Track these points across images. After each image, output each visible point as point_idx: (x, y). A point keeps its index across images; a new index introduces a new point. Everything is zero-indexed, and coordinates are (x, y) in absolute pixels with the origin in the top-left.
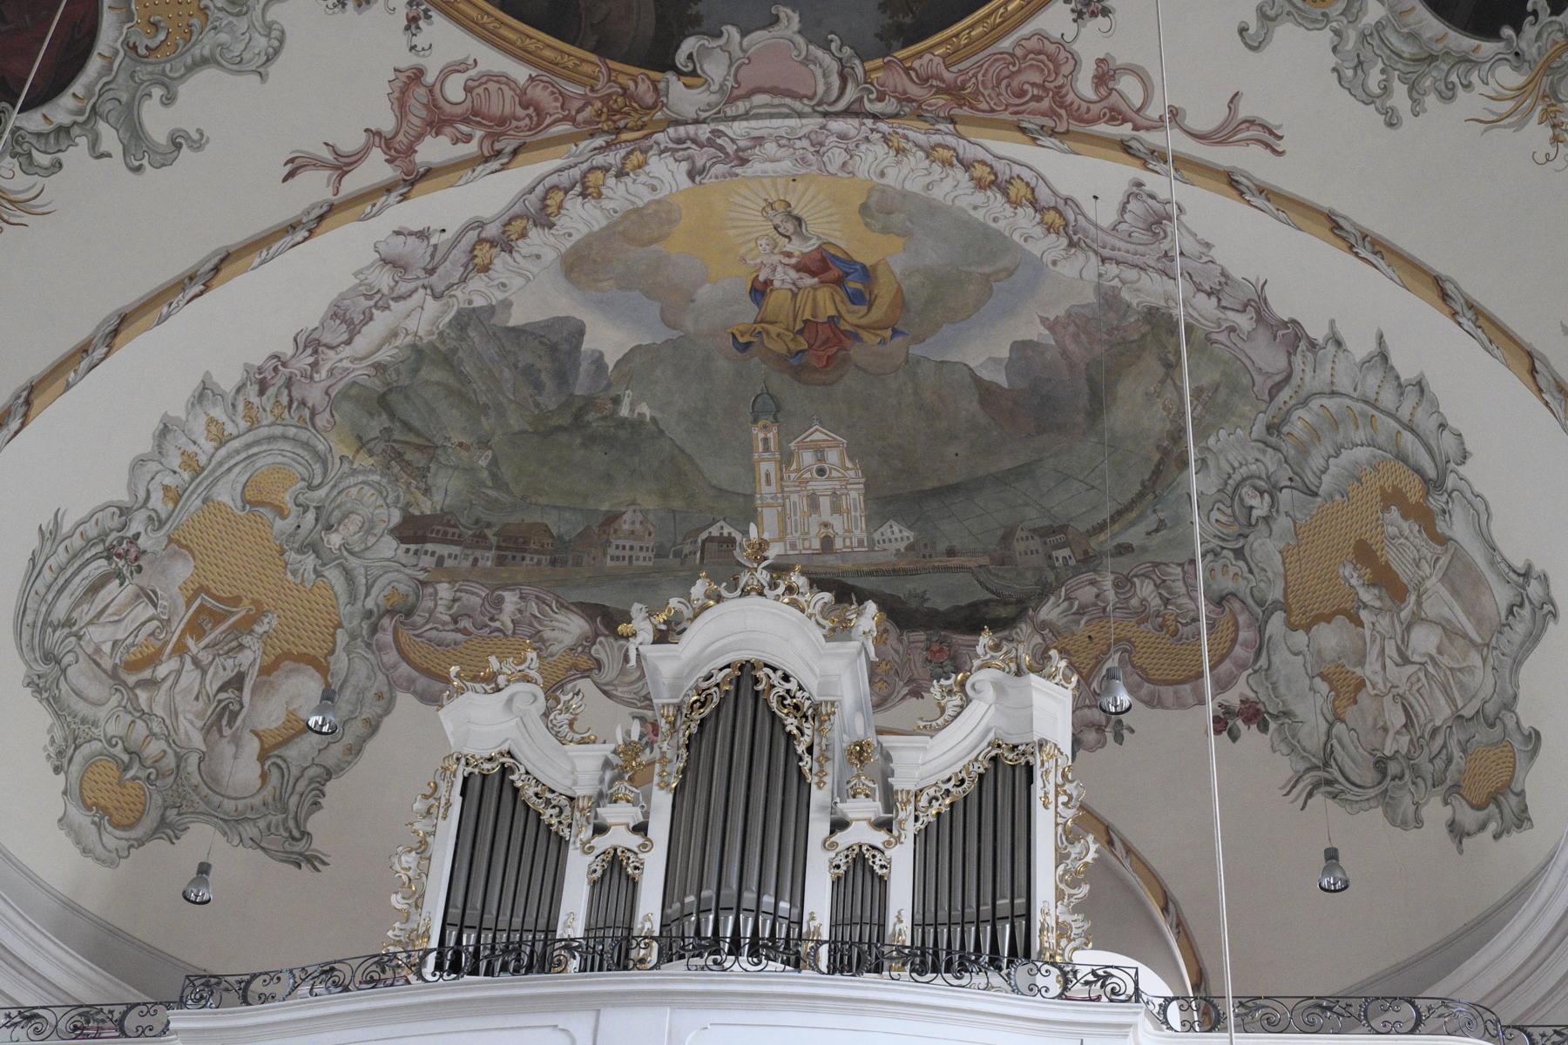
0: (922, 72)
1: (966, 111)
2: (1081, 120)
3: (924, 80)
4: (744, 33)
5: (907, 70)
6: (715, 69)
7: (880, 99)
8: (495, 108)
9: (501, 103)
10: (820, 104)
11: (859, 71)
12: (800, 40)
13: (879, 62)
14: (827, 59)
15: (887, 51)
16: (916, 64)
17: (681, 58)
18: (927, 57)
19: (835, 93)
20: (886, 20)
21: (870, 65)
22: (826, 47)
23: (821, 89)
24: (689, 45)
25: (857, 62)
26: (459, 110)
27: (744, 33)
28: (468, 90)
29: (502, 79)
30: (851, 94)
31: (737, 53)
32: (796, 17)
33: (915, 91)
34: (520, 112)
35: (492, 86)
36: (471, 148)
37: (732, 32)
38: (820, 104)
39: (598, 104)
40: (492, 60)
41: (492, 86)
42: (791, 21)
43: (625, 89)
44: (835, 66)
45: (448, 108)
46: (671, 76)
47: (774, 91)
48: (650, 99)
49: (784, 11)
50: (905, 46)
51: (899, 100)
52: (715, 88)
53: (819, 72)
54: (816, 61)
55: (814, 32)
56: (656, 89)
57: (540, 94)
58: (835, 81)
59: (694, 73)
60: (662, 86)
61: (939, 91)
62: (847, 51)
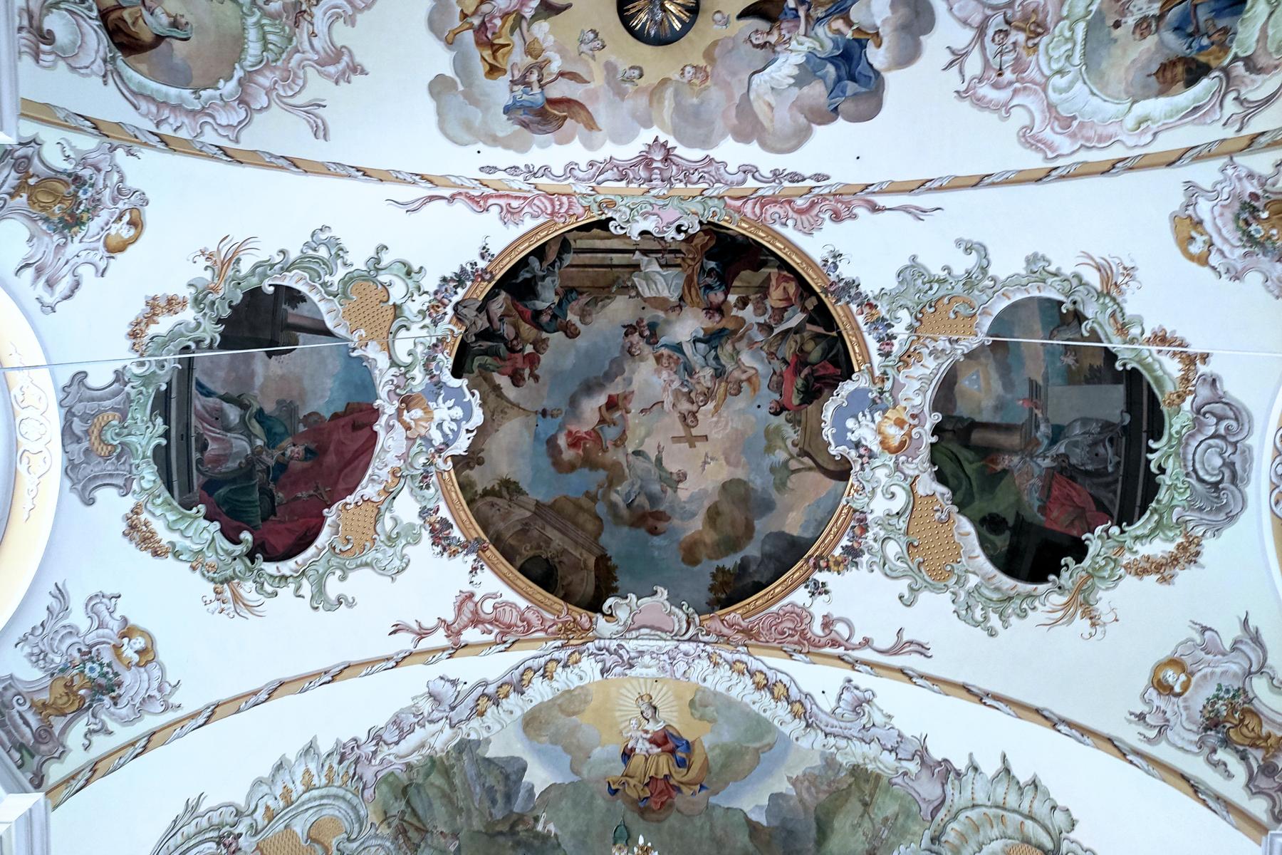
0: (730, 622)
1: (753, 641)
2: (815, 646)
3: (731, 626)
4: (639, 599)
5: (722, 621)
6: (622, 614)
7: (708, 634)
10: (675, 635)
11: (697, 620)
12: (667, 604)
13: (708, 616)
14: (680, 613)
15: (713, 611)
16: (727, 618)
17: (605, 607)
18: (733, 615)
19: (684, 631)
20: (711, 596)
21: (702, 617)
22: (680, 607)
23: (676, 628)
24: (610, 601)
25: (696, 616)
27: (639, 599)
30: (692, 631)
31: (634, 607)
33: (725, 631)
37: (632, 597)
38: (675, 635)
42: (663, 593)
44: (684, 617)
46: (599, 616)
47: (652, 628)
50: (722, 608)
51: (718, 636)
52: (621, 623)
53: (676, 620)
55: (674, 600)
56: (591, 621)
58: (685, 626)
59: (611, 615)
61: (739, 631)
62: (691, 610)
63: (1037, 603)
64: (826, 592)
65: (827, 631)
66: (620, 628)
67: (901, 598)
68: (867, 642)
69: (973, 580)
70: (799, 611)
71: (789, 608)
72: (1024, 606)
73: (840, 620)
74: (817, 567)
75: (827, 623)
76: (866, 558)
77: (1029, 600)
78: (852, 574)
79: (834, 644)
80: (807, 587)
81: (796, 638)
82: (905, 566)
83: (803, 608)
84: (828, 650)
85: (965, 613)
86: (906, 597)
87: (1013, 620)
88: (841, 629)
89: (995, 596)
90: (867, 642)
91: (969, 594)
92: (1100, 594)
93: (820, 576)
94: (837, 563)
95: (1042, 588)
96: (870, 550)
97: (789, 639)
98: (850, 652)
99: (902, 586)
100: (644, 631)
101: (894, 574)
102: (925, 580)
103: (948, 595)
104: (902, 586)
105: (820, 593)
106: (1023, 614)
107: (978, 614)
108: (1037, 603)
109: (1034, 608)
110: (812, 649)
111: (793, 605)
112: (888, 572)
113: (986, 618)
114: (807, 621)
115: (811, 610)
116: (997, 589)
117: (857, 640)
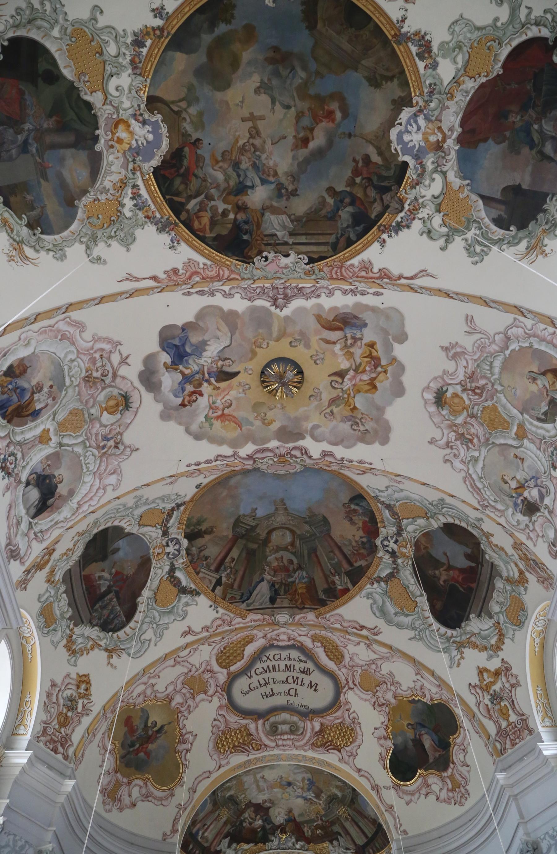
67: (102, 12)
76: (129, 40)
78: (137, 26)
86: (98, 13)
91: (57, 22)
96: (127, 47)
99: (102, 22)
101: (109, 30)
102: (87, 27)
103: (70, 18)
104: (102, 22)
112: (113, 31)
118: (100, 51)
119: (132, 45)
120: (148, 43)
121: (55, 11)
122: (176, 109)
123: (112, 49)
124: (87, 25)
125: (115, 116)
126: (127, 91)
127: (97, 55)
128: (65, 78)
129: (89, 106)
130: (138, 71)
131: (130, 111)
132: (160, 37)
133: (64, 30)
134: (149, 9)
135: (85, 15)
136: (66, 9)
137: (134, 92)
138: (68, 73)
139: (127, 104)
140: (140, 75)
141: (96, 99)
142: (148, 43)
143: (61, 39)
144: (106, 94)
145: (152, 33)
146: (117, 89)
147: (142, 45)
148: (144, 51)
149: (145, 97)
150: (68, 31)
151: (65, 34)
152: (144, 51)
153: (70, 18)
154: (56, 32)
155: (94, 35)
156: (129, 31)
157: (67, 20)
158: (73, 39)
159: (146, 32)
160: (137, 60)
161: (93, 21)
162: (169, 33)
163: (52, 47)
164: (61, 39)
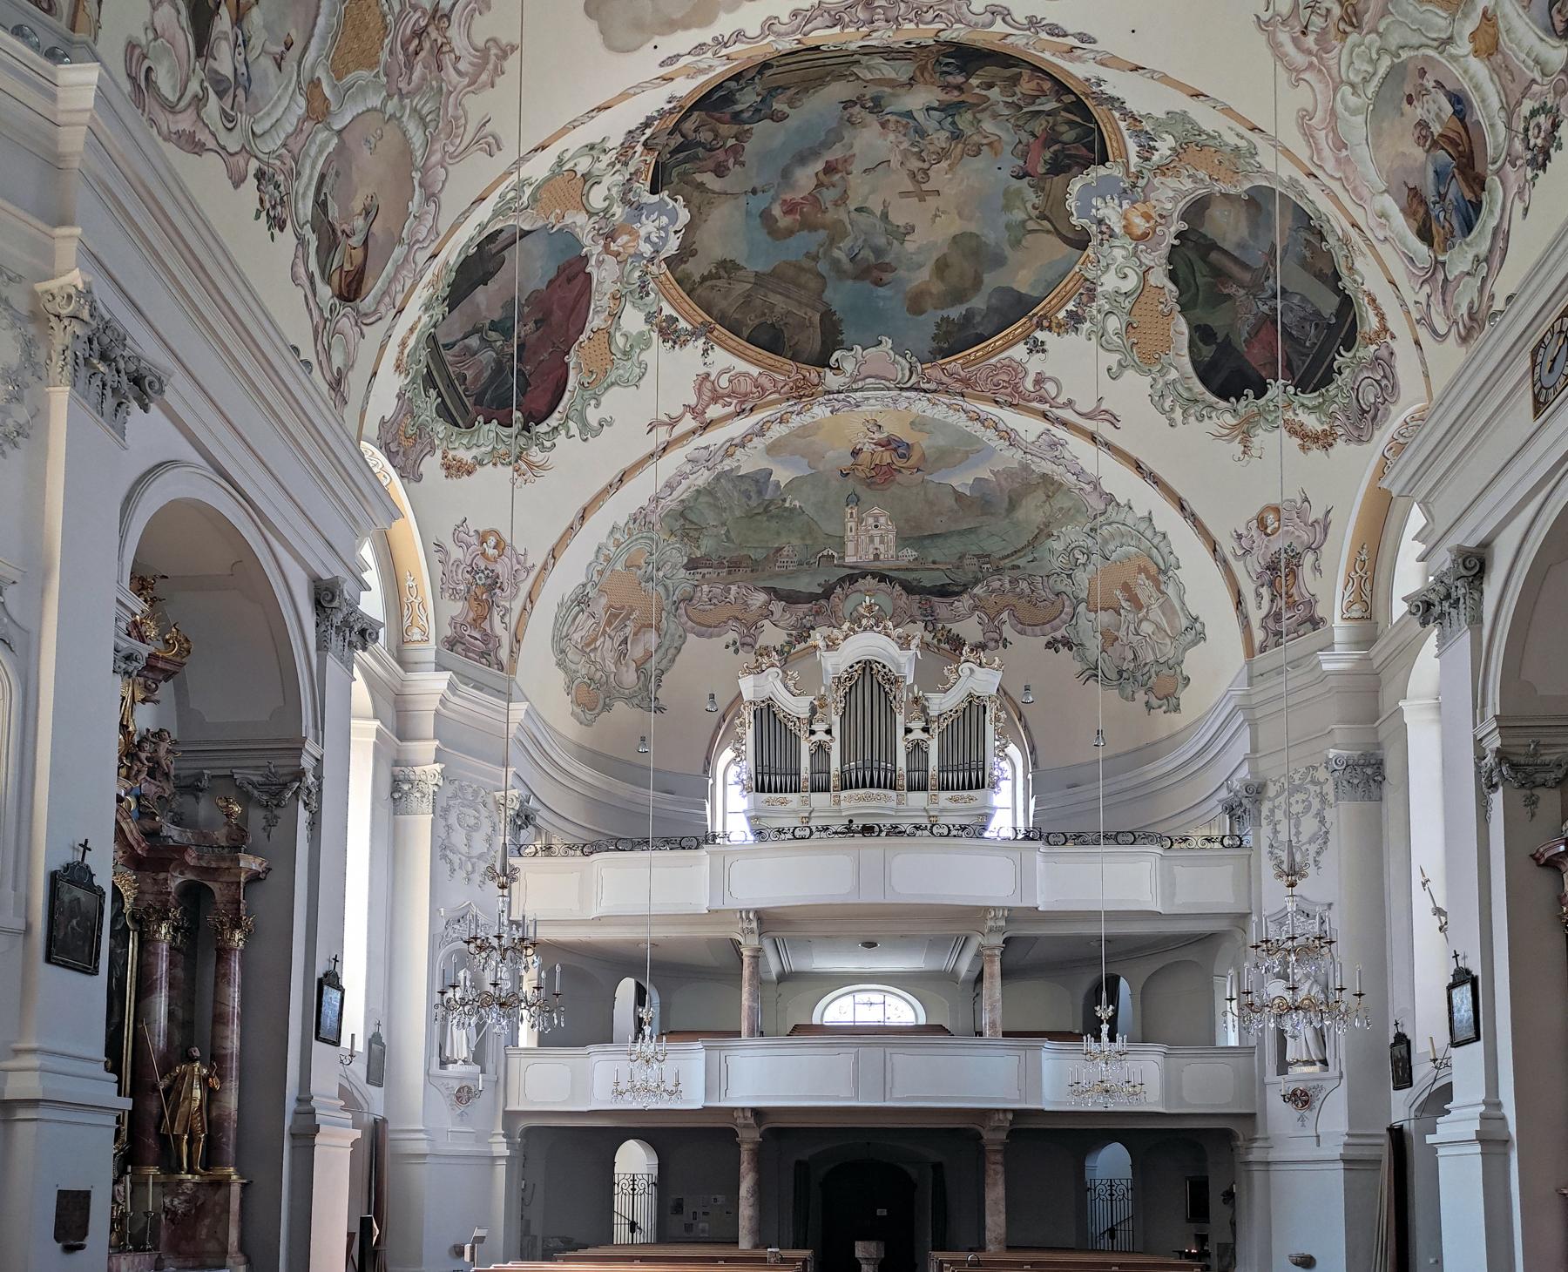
6: (849, 366)
8: (743, 390)
9: (745, 386)
12: (891, 352)
13: (929, 365)
14: (904, 362)
16: (947, 367)
18: (953, 364)
20: (934, 345)
21: (924, 366)
23: (900, 376)
24: (837, 355)
26: (726, 391)
28: (730, 381)
29: (746, 375)
31: (860, 358)
32: (890, 341)
33: (945, 379)
34: (754, 390)
35: (742, 379)
36: (732, 408)
39: (791, 384)
40: (742, 366)
41: (742, 379)
42: (888, 343)
43: (804, 377)
44: (908, 366)
45: (721, 391)
46: (827, 370)
48: (816, 381)
49: (884, 339)
53: (899, 368)
54: (898, 363)
55: (899, 349)
57: (764, 381)
58: (907, 373)
59: (838, 368)
60: (822, 374)
61: (958, 380)
62: (914, 359)
63: (1214, 415)
64: (1044, 351)
65: (1038, 388)
66: (847, 380)
67: (1109, 370)
68: (1070, 403)
69: (1173, 374)
70: (1015, 365)
71: (1006, 362)
72: (1204, 412)
73: (1050, 379)
74: (1040, 326)
75: (1039, 381)
76: (1087, 325)
77: (1209, 409)
79: (1042, 400)
80: (1026, 344)
81: (1009, 389)
82: (1119, 341)
83: (1019, 364)
84: (1035, 404)
85: (1157, 399)
87: (1192, 419)
88: (1050, 388)
89: (1185, 395)
90: (1070, 403)
92: (1260, 431)
93: (1040, 335)
94: (1059, 326)
95: (1223, 404)
97: (1003, 390)
98: (1053, 409)
100: (868, 380)
101: (1109, 347)
103: (1149, 380)
105: (1038, 351)
106: (1200, 419)
107: (1167, 404)
108: (1214, 415)
109: (1210, 418)
110: (1021, 402)
111: (1011, 359)
112: (1104, 344)
113: (1172, 410)
114: (1021, 376)
115: (1027, 366)
116: (1189, 389)
117: (1061, 400)
118: (1130, 327)
119: (1084, 318)
120: (1062, 314)
121: (1162, 395)
122: (1045, 223)
123: (1113, 323)
124: (1133, 363)
125: (1142, 247)
126: (1113, 268)
127: (1135, 325)
128: (1189, 324)
129: (1173, 276)
130: (1087, 284)
131: (1117, 243)
132: (1045, 317)
133: (1163, 372)
134: (1049, 354)
135: (1130, 374)
136: (1150, 391)
137: (1103, 263)
138: (1182, 325)
139: (1119, 253)
140: (1087, 280)
141: (1159, 277)
142: (1062, 314)
143: (1171, 364)
144: (1144, 277)
145: (1053, 325)
146: (1125, 276)
147: (1070, 314)
148: (1070, 306)
149: (1089, 251)
150: (1159, 367)
151: (1163, 367)
152: (1070, 306)
153: (1149, 380)
154: (1173, 374)
155: (1129, 349)
156: (1082, 336)
157: (1154, 379)
158: (1157, 356)
159: (1061, 328)
160: (1085, 299)
161: (1124, 364)
162: (1031, 319)
163: (1186, 361)
164: (1171, 364)
